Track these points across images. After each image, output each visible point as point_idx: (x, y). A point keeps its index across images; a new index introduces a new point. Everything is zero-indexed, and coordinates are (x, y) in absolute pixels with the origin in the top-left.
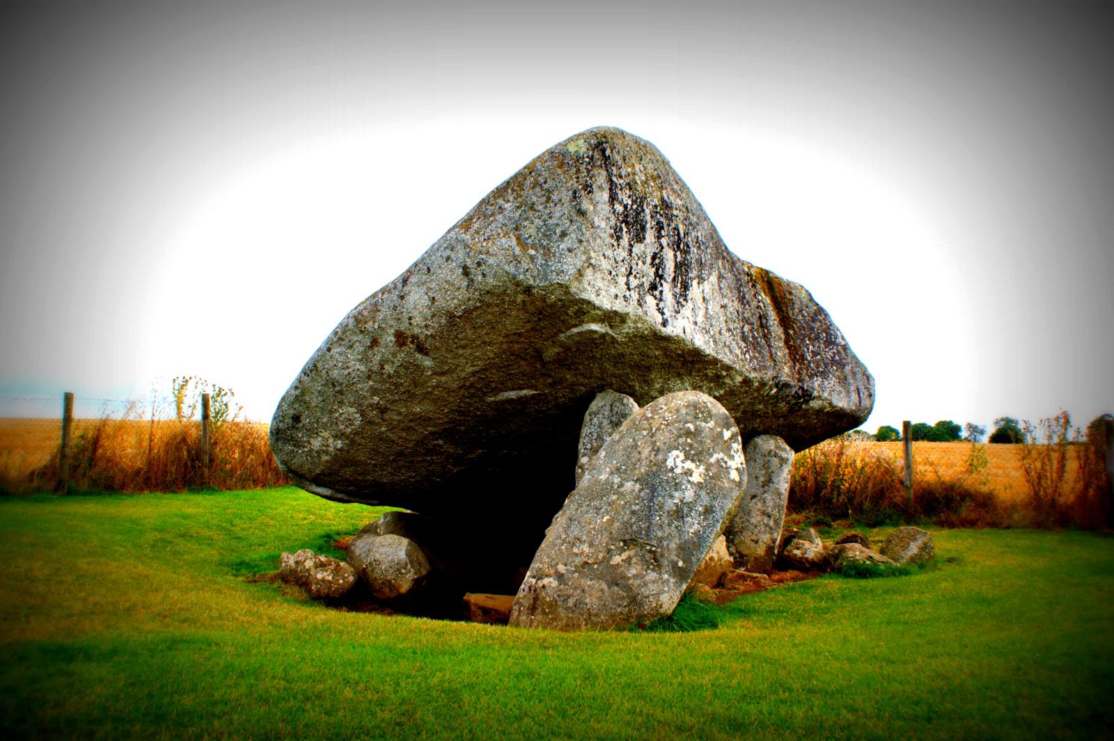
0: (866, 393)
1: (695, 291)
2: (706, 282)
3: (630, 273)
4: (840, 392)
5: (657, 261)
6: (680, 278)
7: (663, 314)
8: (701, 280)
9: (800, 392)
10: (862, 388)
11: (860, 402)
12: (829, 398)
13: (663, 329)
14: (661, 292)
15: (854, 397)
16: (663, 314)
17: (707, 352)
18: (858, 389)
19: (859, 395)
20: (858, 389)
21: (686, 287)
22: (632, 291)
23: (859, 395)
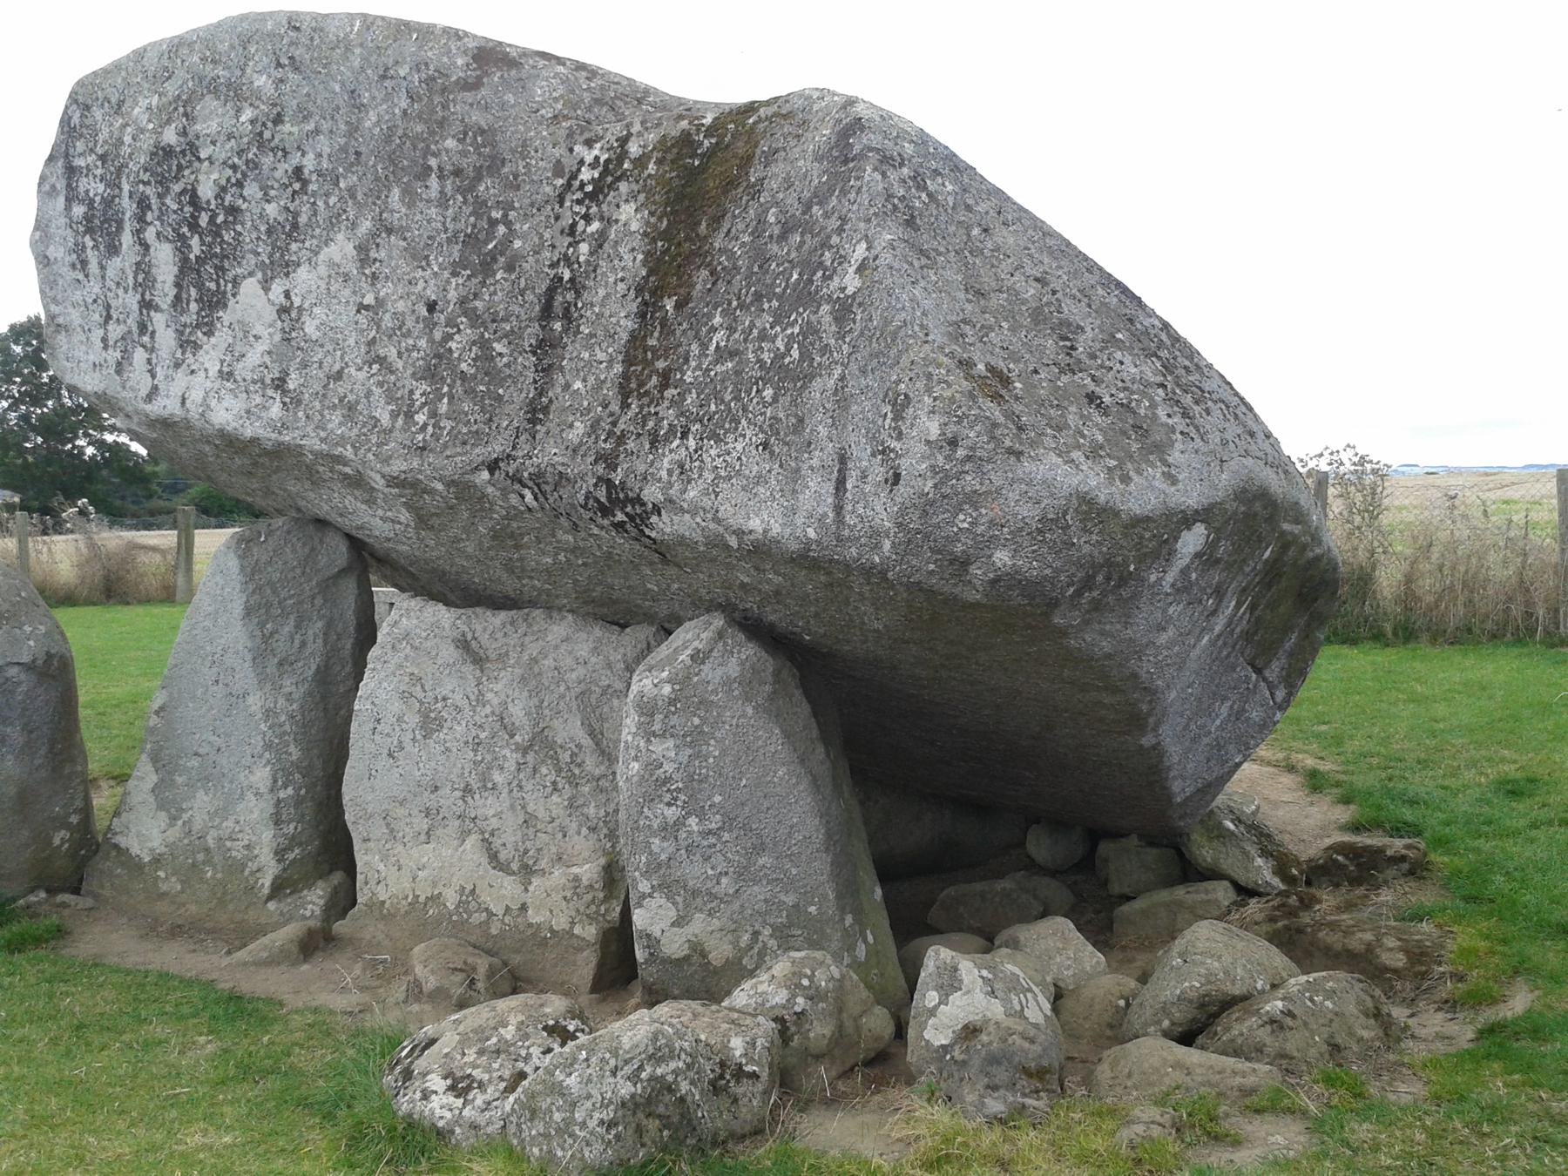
0: (878, 472)
1: (252, 301)
2: (303, 273)
3: (109, 317)
4: (760, 479)
5: (144, 273)
6: (193, 292)
7: (153, 376)
8: (280, 265)
9: (602, 494)
10: (861, 454)
11: (839, 509)
12: (707, 502)
13: (148, 408)
14: (153, 332)
15: (816, 492)
16: (153, 376)
17: (248, 433)
18: (843, 460)
19: (840, 485)
20: (843, 460)
21: (214, 302)
22: (110, 351)
23: (840, 485)
